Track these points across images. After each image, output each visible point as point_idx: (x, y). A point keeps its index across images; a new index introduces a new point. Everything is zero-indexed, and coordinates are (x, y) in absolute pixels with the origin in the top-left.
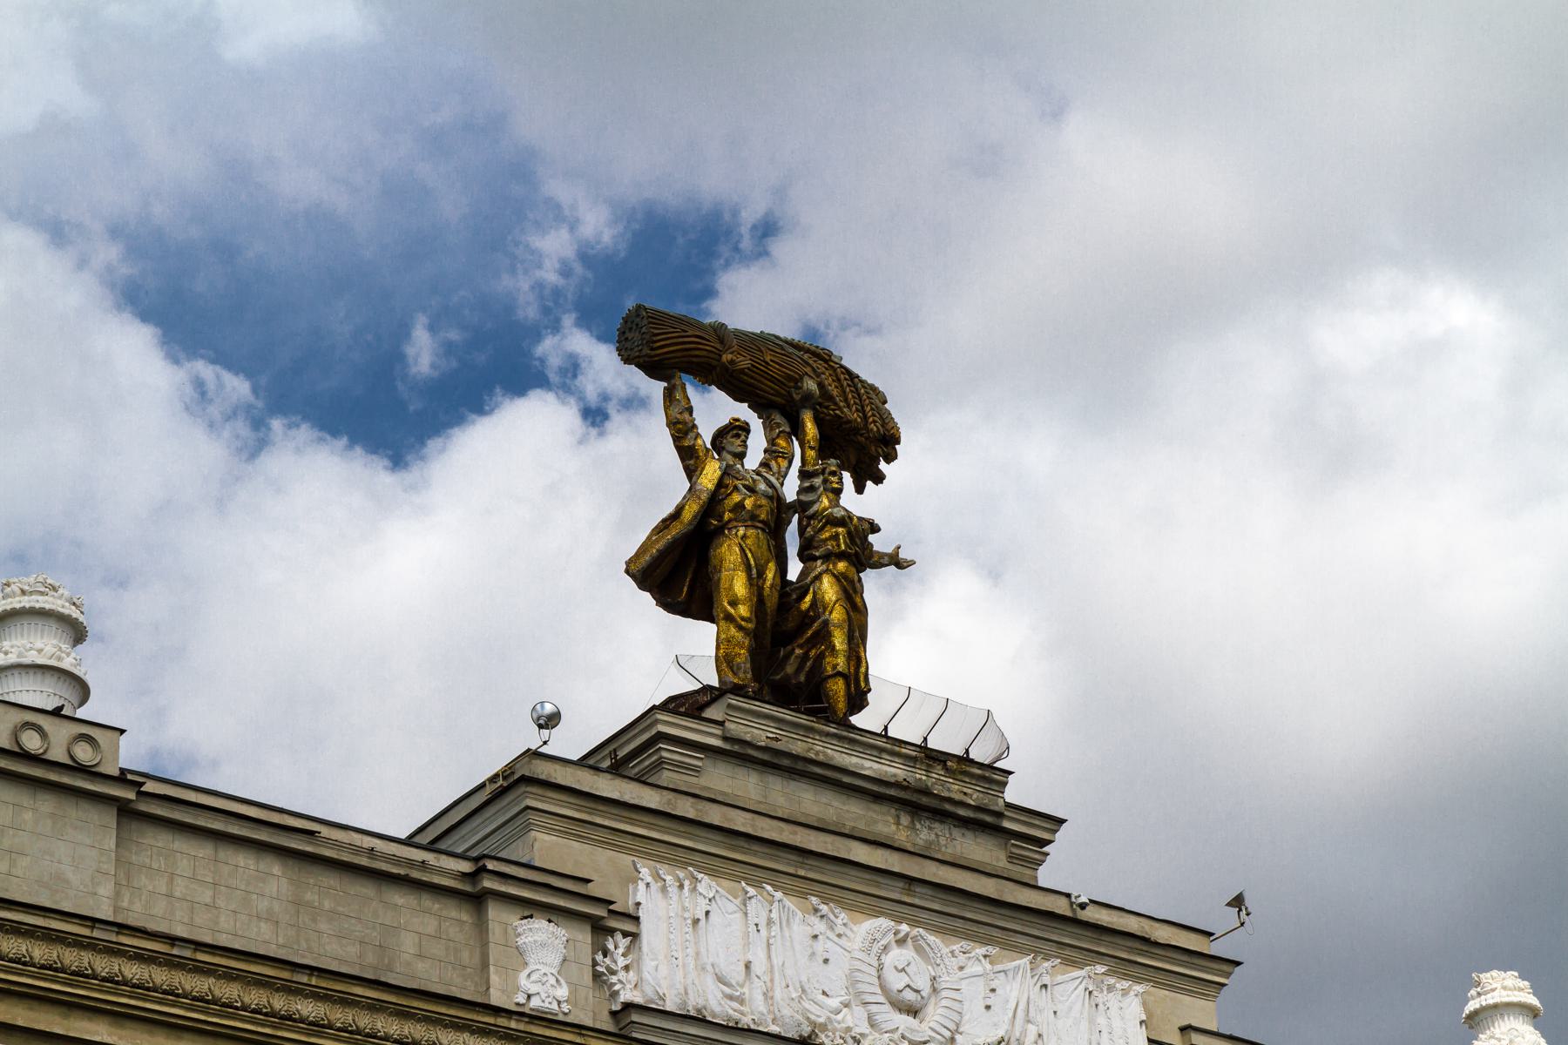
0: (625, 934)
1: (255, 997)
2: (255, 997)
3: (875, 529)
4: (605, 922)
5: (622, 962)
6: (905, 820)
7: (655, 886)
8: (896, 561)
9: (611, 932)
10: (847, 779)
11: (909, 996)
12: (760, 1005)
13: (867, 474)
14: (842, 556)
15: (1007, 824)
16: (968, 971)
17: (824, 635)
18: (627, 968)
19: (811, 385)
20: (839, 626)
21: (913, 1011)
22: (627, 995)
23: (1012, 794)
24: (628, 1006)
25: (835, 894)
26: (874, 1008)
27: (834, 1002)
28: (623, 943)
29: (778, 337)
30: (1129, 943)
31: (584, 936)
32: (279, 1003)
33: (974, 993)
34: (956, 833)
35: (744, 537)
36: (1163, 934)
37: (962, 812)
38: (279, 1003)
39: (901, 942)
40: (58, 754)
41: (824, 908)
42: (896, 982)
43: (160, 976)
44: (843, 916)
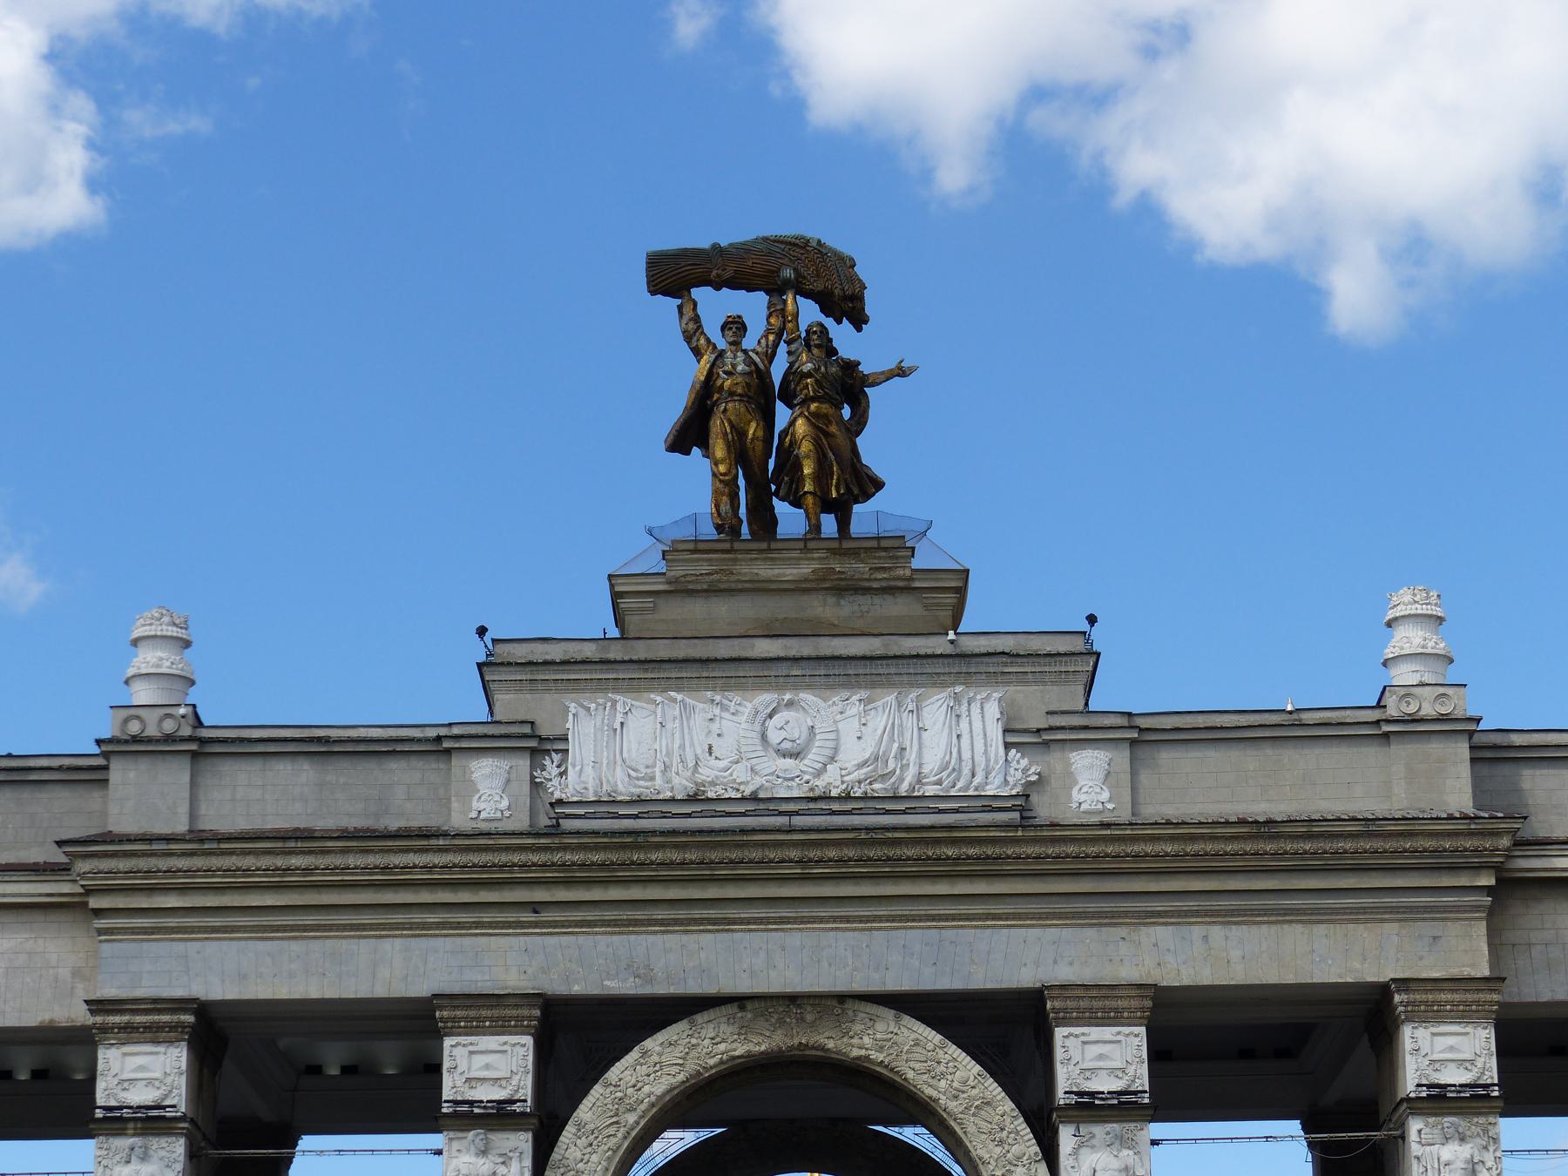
0: (557, 751)
1: (265, 862)
2: (265, 862)
3: (850, 367)
4: (540, 746)
5: (555, 771)
6: (831, 600)
7: (582, 712)
8: (901, 372)
9: (548, 752)
10: (773, 586)
11: (786, 745)
12: (659, 781)
13: (859, 321)
14: (813, 399)
15: (917, 584)
16: (848, 713)
17: (798, 467)
18: (561, 774)
19: (788, 273)
20: (807, 456)
21: (796, 755)
22: (557, 795)
23: (916, 563)
24: (560, 802)
25: (728, 684)
26: (754, 762)
27: (722, 764)
28: (556, 757)
29: (765, 239)
30: (995, 660)
31: (523, 763)
32: (280, 862)
33: (849, 728)
34: (877, 600)
35: (725, 410)
36: (1036, 644)
37: (875, 585)
38: (280, 862)
39: (790, 704)
40: (151, 731)
41: (718, 698)
42: (774, 737)
43: (198, 862)
44: (738, 699)
